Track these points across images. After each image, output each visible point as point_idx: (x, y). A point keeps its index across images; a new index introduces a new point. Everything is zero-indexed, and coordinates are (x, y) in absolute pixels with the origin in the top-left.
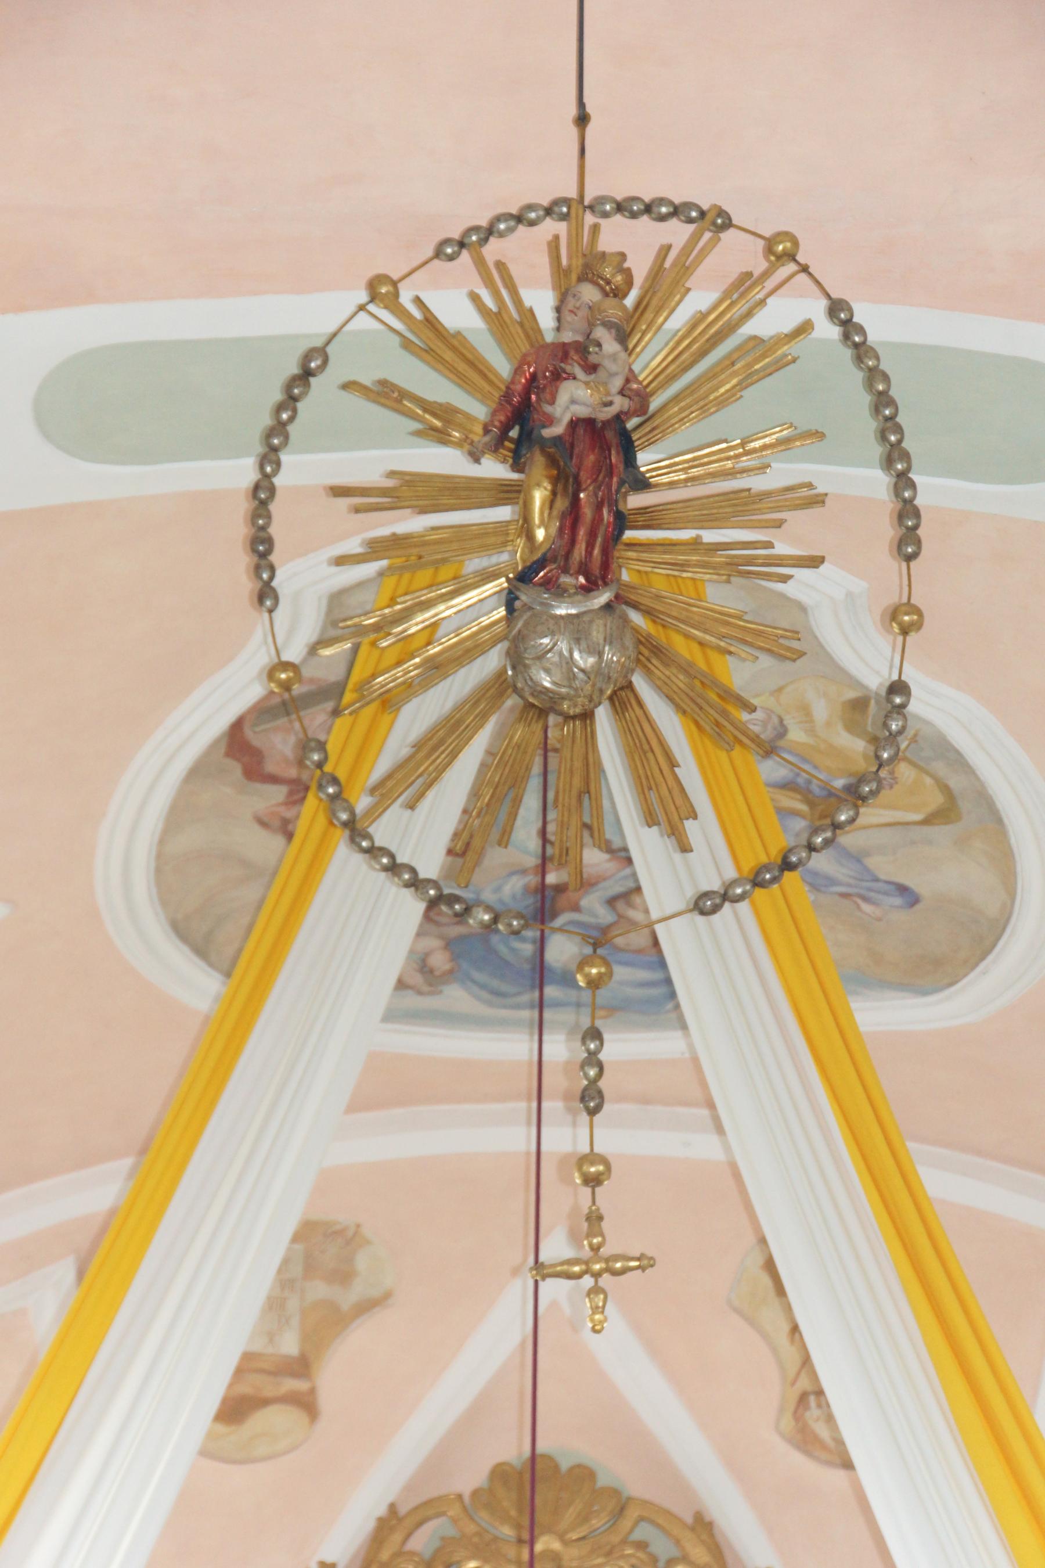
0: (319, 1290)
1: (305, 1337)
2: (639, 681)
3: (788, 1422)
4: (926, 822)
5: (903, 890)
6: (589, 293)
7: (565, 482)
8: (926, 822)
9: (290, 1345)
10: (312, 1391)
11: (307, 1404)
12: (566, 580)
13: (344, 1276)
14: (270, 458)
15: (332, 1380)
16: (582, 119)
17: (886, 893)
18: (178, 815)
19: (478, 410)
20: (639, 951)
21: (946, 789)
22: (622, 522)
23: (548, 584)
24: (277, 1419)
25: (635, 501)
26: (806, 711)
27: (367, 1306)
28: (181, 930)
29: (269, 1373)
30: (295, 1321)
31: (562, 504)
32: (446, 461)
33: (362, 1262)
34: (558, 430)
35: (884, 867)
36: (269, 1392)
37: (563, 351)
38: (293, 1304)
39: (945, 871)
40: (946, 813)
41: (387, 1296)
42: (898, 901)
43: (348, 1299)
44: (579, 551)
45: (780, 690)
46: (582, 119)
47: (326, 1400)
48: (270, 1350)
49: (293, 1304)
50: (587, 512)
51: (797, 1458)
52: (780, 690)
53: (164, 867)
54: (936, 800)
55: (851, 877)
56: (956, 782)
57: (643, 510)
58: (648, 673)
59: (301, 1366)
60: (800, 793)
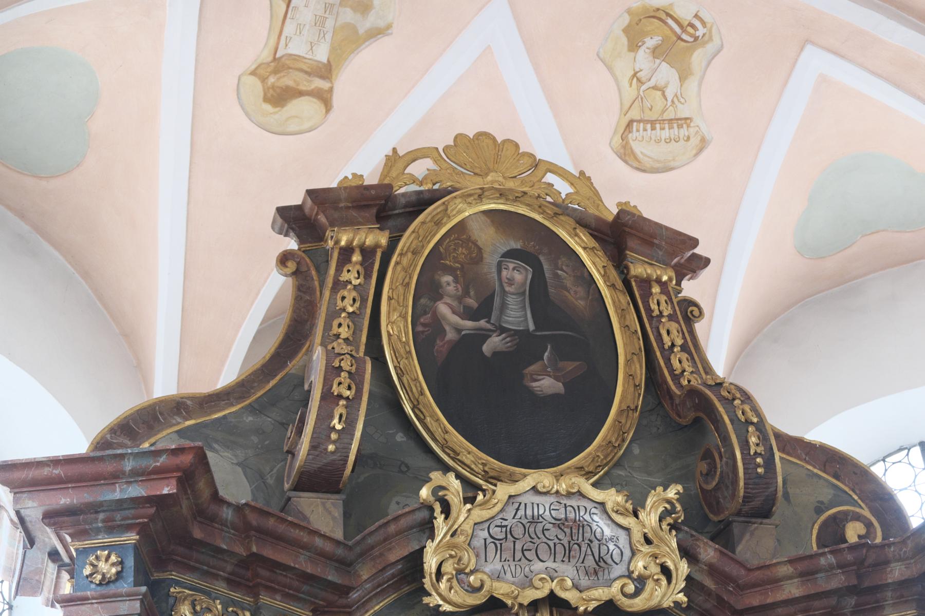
0: (348, 15)
1: (333, 50)
3: (617, 140)
9: (322, 54)
10: (331, 90)
11: (325, 99)
13: (364, 8)
24: (305, 107)
27: (377, 33)
29: (306, 72)
30: (328, 37)
36: (302, 88)
41: (389, 27)
47: (337, 100)
49: (330, 24)
59: (326, 71)
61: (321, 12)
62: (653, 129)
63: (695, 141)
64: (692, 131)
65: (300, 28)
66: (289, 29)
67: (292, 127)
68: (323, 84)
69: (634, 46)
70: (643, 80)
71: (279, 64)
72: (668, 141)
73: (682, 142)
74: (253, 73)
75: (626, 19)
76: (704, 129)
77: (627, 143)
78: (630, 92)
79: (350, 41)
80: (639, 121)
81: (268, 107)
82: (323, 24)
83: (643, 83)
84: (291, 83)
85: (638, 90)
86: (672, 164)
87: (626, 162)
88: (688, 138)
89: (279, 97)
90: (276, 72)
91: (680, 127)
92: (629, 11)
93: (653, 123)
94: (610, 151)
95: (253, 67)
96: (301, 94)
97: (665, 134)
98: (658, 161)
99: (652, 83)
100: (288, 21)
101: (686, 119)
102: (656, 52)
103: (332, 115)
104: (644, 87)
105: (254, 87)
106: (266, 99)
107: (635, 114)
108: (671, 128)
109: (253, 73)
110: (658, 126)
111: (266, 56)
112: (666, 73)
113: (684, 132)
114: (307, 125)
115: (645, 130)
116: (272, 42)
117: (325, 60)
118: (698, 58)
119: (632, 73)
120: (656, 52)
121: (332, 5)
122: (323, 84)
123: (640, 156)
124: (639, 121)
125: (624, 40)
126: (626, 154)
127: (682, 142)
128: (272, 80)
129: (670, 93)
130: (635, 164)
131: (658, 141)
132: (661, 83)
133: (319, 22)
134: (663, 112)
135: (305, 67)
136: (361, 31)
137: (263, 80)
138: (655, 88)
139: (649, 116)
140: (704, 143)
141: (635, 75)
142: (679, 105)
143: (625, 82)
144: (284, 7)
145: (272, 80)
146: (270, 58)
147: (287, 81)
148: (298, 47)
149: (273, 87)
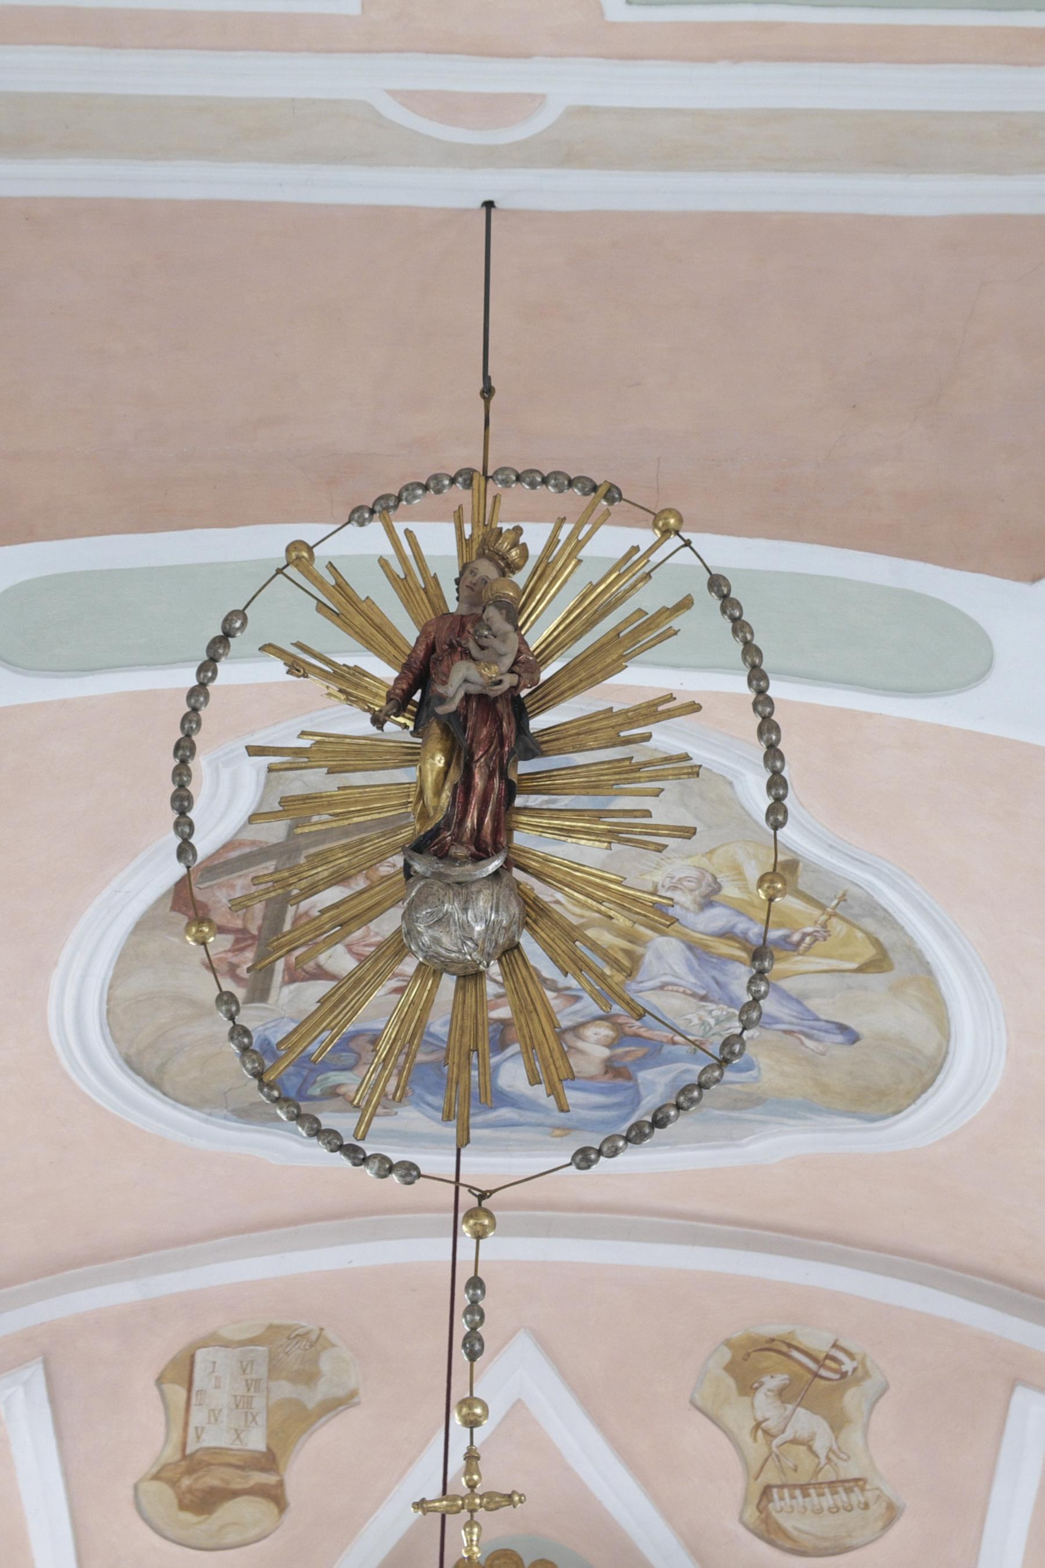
0: (284, 1389)
1: (272, 1434)
2: (525, 940)
3: (752, 1514)
4: (860, 970)
5: (843, 1029)
6: (487, 569)
7: (460, 755)
8: (860, 970)
9: (256, 1441)
10: (281, 1484)
11: (276, 1497)
12: (460, 851)
13: (309, 1377)
14: (208, 668)
15: (299, 1474)
16: (488, 392)
17: (826, 1031)
18: (127, 961)
19: (386, 673)
20: (592, 1078)
21: (876, 943)
22: (511, 790)
23: (443, 855)
24: (245, 1511)
25: (524, 767)
26: (738, 872)
27: (333, 1406)
28: (133, 1064)
30: (261, 1419)
31: (455, 775)
32: (356, 724)
33: (325, 1364)
34: (452, 707)
35: (825, 1008)
36: (237, 1484)
37: (460, 622)
38: (259, 1403)
39: (882, 1013)
40: (879, 962)
41: (353, 1394)
42: (840, 1038)
43: (314, 1397)
44: (471, 821)
45: (712, 852)
46: (488, 392)
48: (237, 1446)
49: (259, 1403)
50: (479, 781)
51: (762, 1547)
52: (712, 852)
53: (116, 1014)
54: (869, 952)
55: (789, 1015)
56: (885, 936)
57: (532, 776)
58: (533, 933)
60: (739, 942)
61: (242, 1390)
62: (806, 1495)
63: (877, 1509)
64: (870, 1495)
65: (214, 1415)
66: (198, 1417)
67: (231, 1538)
68: (271, 1479)
69: (747, 1387)
70: (773, 1431)
71: (192, 1462)
72: (835, 1510)
73: (857, 1512)
74: (156, 1477)
75: (727, 1355)
76: (888, 1491)
77: (769, 1516)
78: (756, 1450)
79: (294, 1422)
80: (781, 1487)
81: (188, 1517)
82: (249, 1404)
83: (774, 1436)
84: (216, 1483)
85: (769, 1446)
86: (849, 1542)
87: (771, 1543)
88: (866, 1506)
89: (205, 1502)
90: (190, 1471)
91: (849, 1491)
92: (728, 1343)
93: (804, 1489)
94: (741, 1530)
95: (154, 1470)
96: (235, 1494)
97: (828, 1501)
98: (824, 1539)
99: (788, 1435)
100: (194, 1408)
101: (856, 1480)
102: (782, 1394)
103: (290, 1516)
104: (776, 1442)
105: (162, 1495)
106: (183, 1507)
107: (771, 1476)
108: (834, 1493)
109: (156, 1477)
110: (812, 1491)
111: (171, 1454)
112: (805, 1421)
113: (857, 1497)
114: (253, 1533)
115: (793, 1497)
116: (176, 1436)
117: (262, 1447)
118: (852, 1399)
119: (754, 1423)
120: (782, 1394)
121: (258, 1381)
122: (271, 1479)
123: (795, 1534)
124: (781, 1487)
125: (730, 1382)
126: (769, 1532)
127: (857, 1512)
128: (186, 1482)
129: (821, 1445)
130: (789, 1545)
131: (819, 1511)
132: (804, 1434)
133: (242, 1404)
134: (817, 1471)
135: (233, 1461)
136: (311, 1406)
137: (173, 1483)
138: (794, 1441)
139: (792, 1478)
140: (892, 1513)
141: (758, 1425)
142: (841, 1463)
143: (746, 1437)
144: (182, 1393)
145: (186, 1482)
146: (178, 1456)
147: (212, 1480)
148: (216, 1438)
149: (190, 1490)
